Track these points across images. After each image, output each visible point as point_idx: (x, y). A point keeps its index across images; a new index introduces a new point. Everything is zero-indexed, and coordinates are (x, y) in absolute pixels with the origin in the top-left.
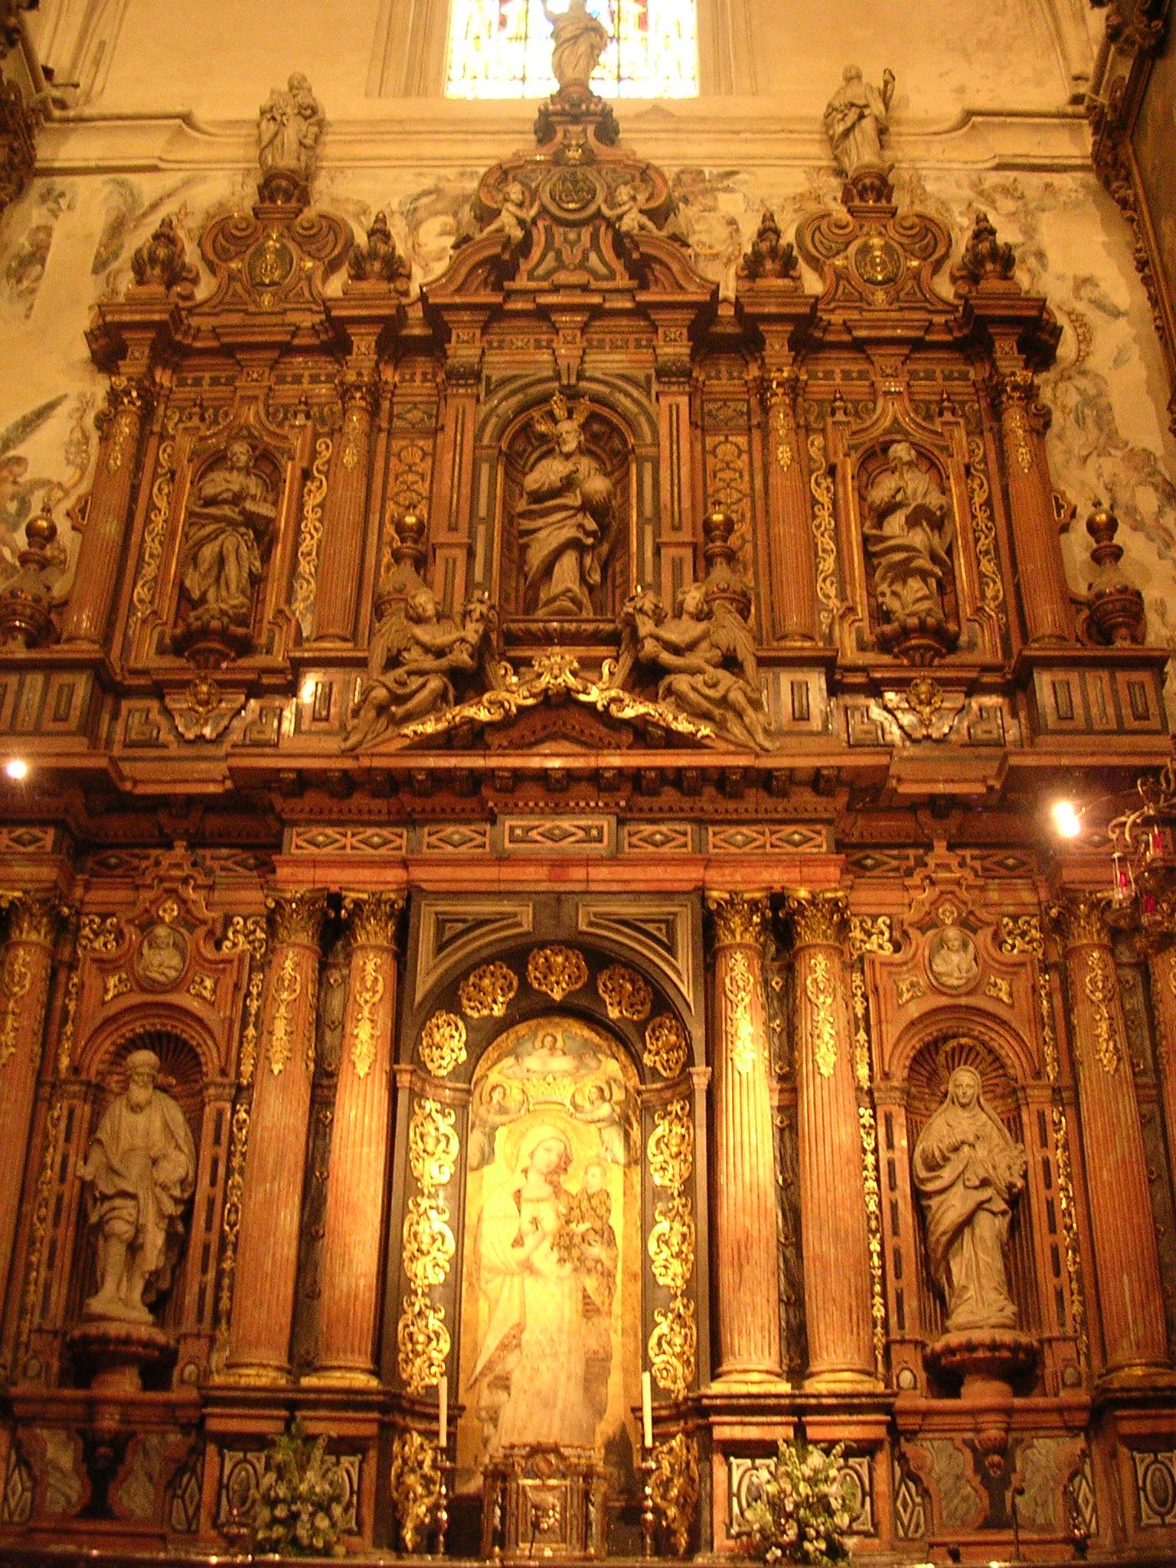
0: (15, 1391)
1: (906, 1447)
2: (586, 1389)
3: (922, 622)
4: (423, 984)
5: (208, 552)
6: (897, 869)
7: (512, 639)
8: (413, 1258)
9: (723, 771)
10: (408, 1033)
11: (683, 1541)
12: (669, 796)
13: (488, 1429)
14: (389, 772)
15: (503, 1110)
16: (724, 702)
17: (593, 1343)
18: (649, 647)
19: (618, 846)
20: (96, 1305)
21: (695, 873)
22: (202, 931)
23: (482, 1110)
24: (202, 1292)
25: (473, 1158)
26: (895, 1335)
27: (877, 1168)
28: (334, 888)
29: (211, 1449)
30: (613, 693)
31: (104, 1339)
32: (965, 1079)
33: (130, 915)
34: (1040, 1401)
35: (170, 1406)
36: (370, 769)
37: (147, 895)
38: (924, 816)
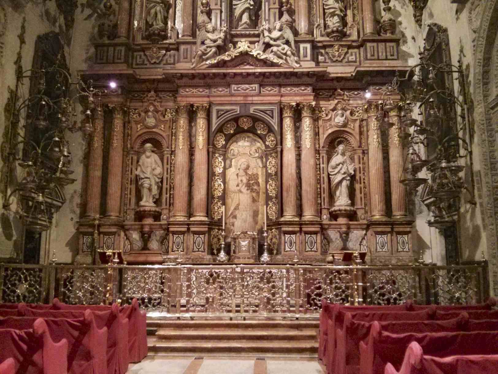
0: (124, 223)
1: (324, 232)
2: (254, 218)
3: (337, 29)
4: (214, 127)
5: (153, 11)
6: (327, 95)
7: (233, 36)
8: (214, 191)
9: (285, 72)
10: (211, 139)
12: (272, 79)
13: (232, 228)
14: (203, 74)
15: (234, 155)
16: (285, 54)
17: (255, 208)
18: (267, 40)
19: (260, 92)
20: (142, 203)
21: (278, 98)
22: (160, 113)
23: (229, 155)
24: (166, 199)
25: (227, 166)
26: (323, 207)
27: (320, 169)
28: (192, 103)
29: (171, 235)
30: (258, 52)
31: (145, 211)
32: (341, 148)
33: (141, 109)
34: (355, 223)
35: (161, 225)
36: (199, 73)
37: (146, 104)
38: (335, 82)
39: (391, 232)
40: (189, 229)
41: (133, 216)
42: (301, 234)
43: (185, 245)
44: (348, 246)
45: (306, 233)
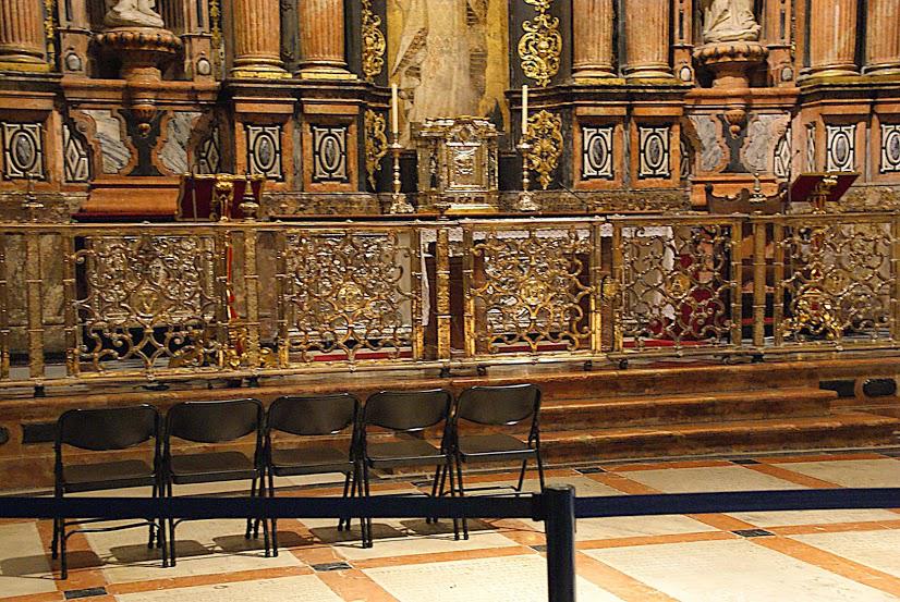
2: (471, 76)
11: (546, 180)
17: (475, 44)
29: (239, 126)
31: (140, 41)
34: (768, 90)
39: (867, 119)
40: (299, 107)
41: (85, 59)
42: (626, 128)
43: (284, 158)
44: (742, 160)
45: (644, 122)
